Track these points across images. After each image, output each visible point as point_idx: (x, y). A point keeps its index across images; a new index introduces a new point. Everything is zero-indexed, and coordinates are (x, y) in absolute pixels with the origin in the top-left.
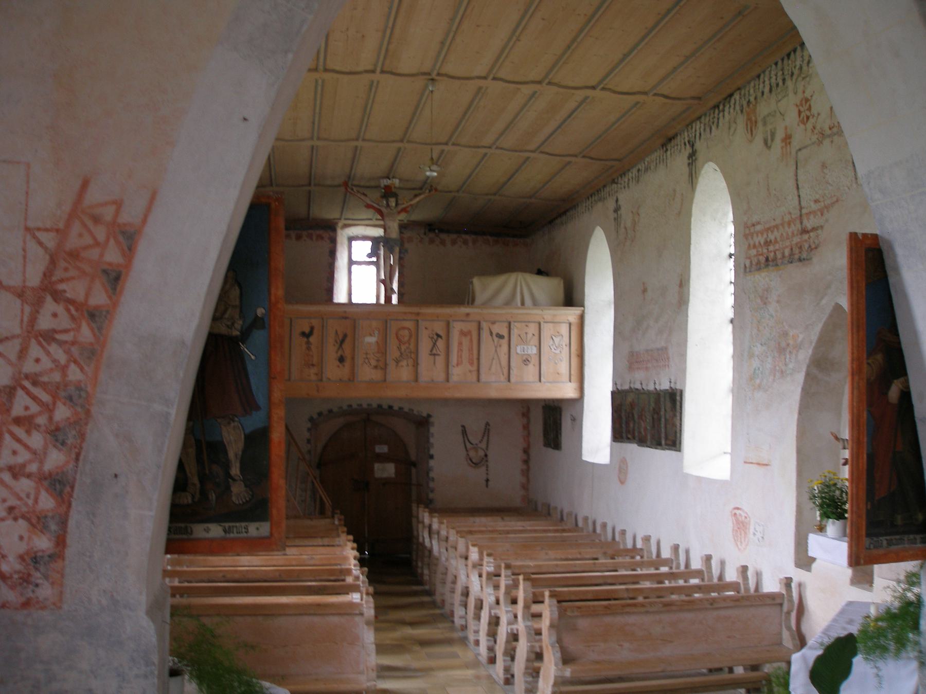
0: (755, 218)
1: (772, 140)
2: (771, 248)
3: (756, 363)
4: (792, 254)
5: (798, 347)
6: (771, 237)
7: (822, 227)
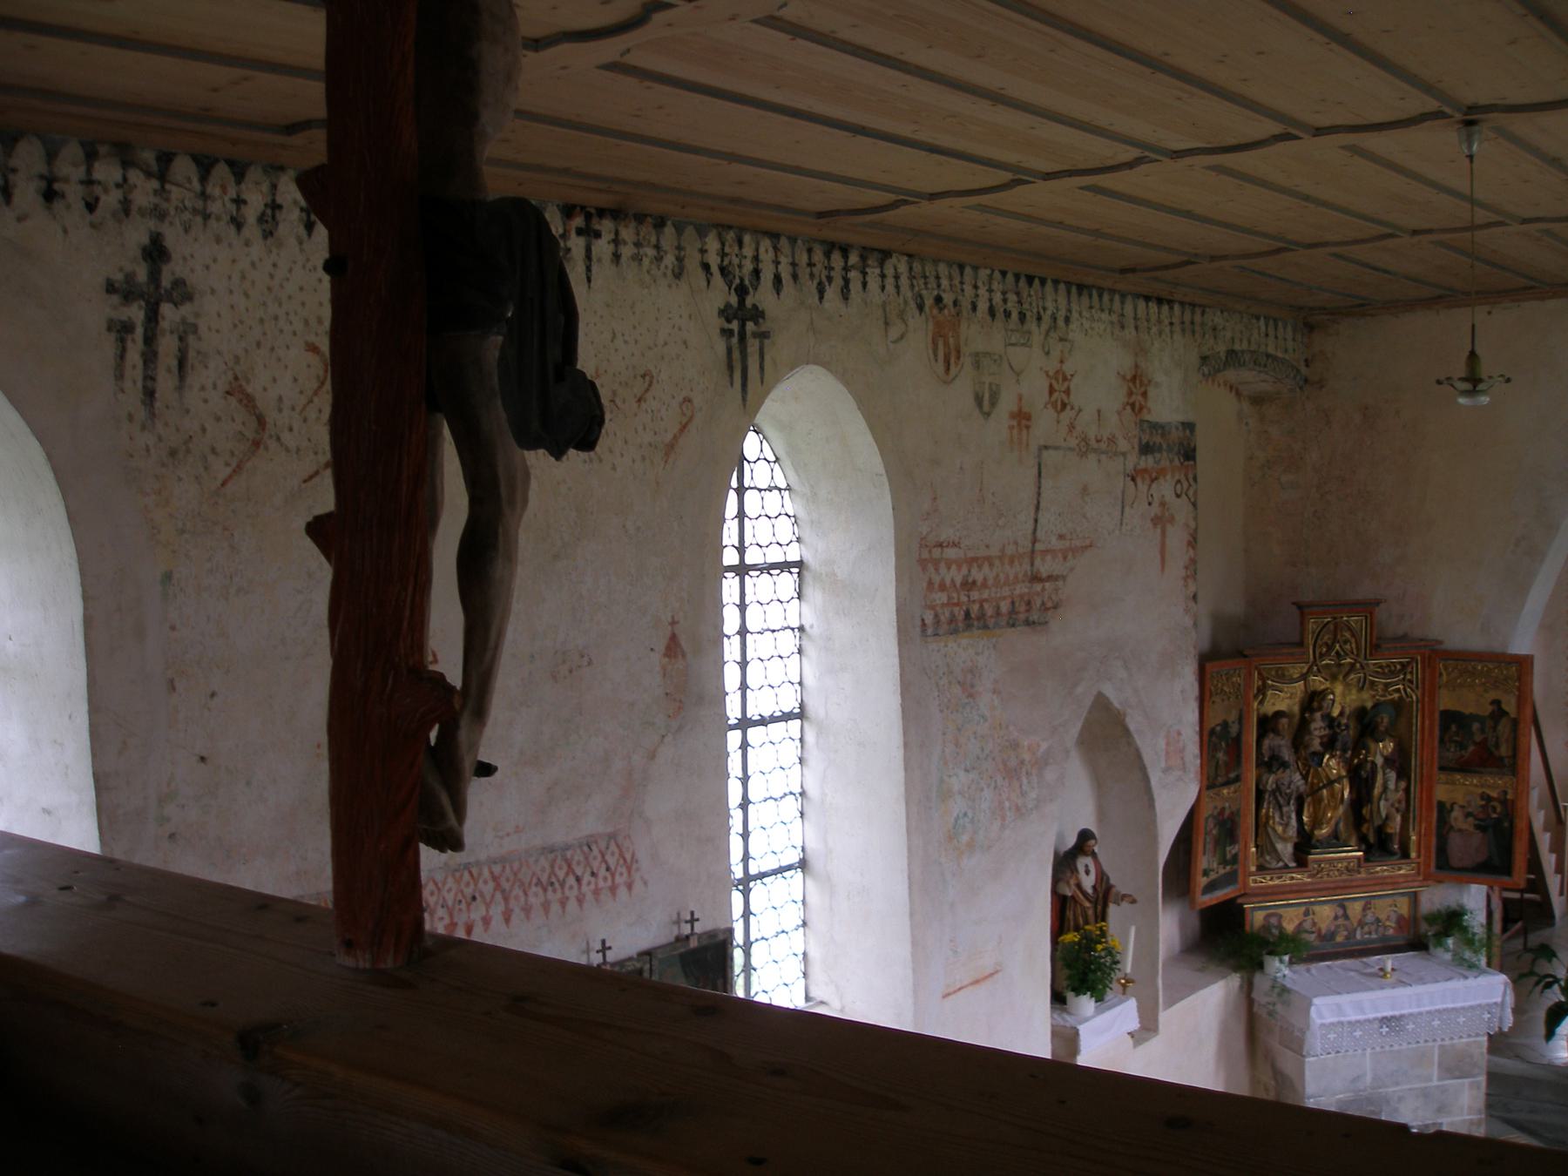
0: (946, 534)
1: (993, 404)
2: (975, 595)
3: (958, 805)
4: (1013, 611)
6: (977, 575)
7: (1064, 578)
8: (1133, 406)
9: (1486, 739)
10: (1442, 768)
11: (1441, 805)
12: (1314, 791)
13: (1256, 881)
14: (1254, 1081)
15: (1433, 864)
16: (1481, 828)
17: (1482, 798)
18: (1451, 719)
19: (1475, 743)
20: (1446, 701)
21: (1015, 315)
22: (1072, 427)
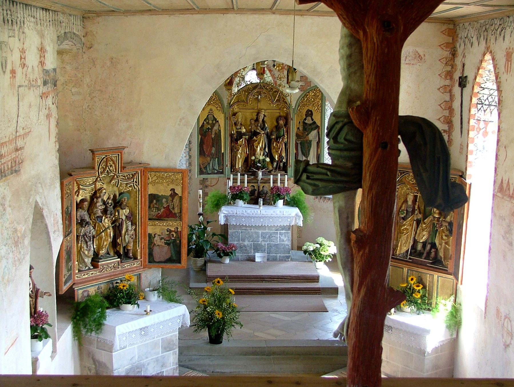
1: (6, 67)
5: (24, 236)
7: (23, 147)
8: (41, 62)
9: (169, 206)
10: (149, 219)
11: (150, 235)
12: (99, 234)
13: (77, 277)
14: (82, 367)
15: (147, 261)
16: (168, 244)
17: (168, 231)
18: (153, 197)
19: (164, 208)
20: (151, 190)
21: (10, 22)
22: (26, 75)
